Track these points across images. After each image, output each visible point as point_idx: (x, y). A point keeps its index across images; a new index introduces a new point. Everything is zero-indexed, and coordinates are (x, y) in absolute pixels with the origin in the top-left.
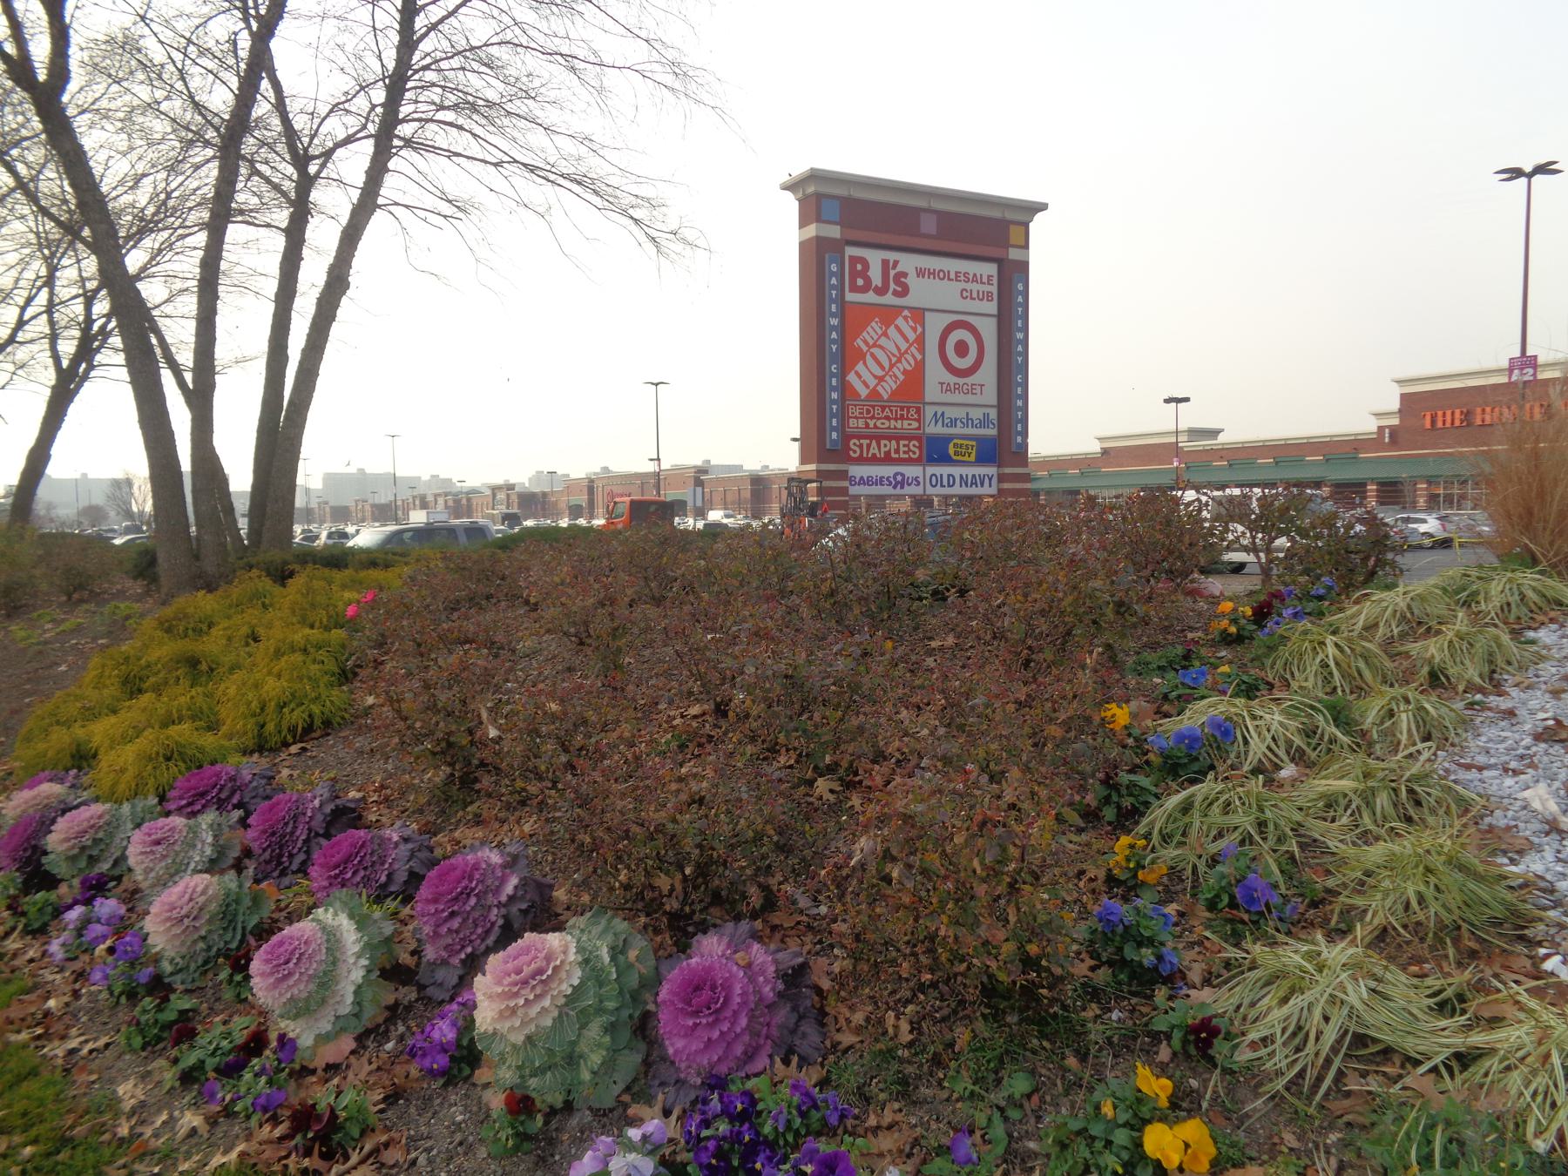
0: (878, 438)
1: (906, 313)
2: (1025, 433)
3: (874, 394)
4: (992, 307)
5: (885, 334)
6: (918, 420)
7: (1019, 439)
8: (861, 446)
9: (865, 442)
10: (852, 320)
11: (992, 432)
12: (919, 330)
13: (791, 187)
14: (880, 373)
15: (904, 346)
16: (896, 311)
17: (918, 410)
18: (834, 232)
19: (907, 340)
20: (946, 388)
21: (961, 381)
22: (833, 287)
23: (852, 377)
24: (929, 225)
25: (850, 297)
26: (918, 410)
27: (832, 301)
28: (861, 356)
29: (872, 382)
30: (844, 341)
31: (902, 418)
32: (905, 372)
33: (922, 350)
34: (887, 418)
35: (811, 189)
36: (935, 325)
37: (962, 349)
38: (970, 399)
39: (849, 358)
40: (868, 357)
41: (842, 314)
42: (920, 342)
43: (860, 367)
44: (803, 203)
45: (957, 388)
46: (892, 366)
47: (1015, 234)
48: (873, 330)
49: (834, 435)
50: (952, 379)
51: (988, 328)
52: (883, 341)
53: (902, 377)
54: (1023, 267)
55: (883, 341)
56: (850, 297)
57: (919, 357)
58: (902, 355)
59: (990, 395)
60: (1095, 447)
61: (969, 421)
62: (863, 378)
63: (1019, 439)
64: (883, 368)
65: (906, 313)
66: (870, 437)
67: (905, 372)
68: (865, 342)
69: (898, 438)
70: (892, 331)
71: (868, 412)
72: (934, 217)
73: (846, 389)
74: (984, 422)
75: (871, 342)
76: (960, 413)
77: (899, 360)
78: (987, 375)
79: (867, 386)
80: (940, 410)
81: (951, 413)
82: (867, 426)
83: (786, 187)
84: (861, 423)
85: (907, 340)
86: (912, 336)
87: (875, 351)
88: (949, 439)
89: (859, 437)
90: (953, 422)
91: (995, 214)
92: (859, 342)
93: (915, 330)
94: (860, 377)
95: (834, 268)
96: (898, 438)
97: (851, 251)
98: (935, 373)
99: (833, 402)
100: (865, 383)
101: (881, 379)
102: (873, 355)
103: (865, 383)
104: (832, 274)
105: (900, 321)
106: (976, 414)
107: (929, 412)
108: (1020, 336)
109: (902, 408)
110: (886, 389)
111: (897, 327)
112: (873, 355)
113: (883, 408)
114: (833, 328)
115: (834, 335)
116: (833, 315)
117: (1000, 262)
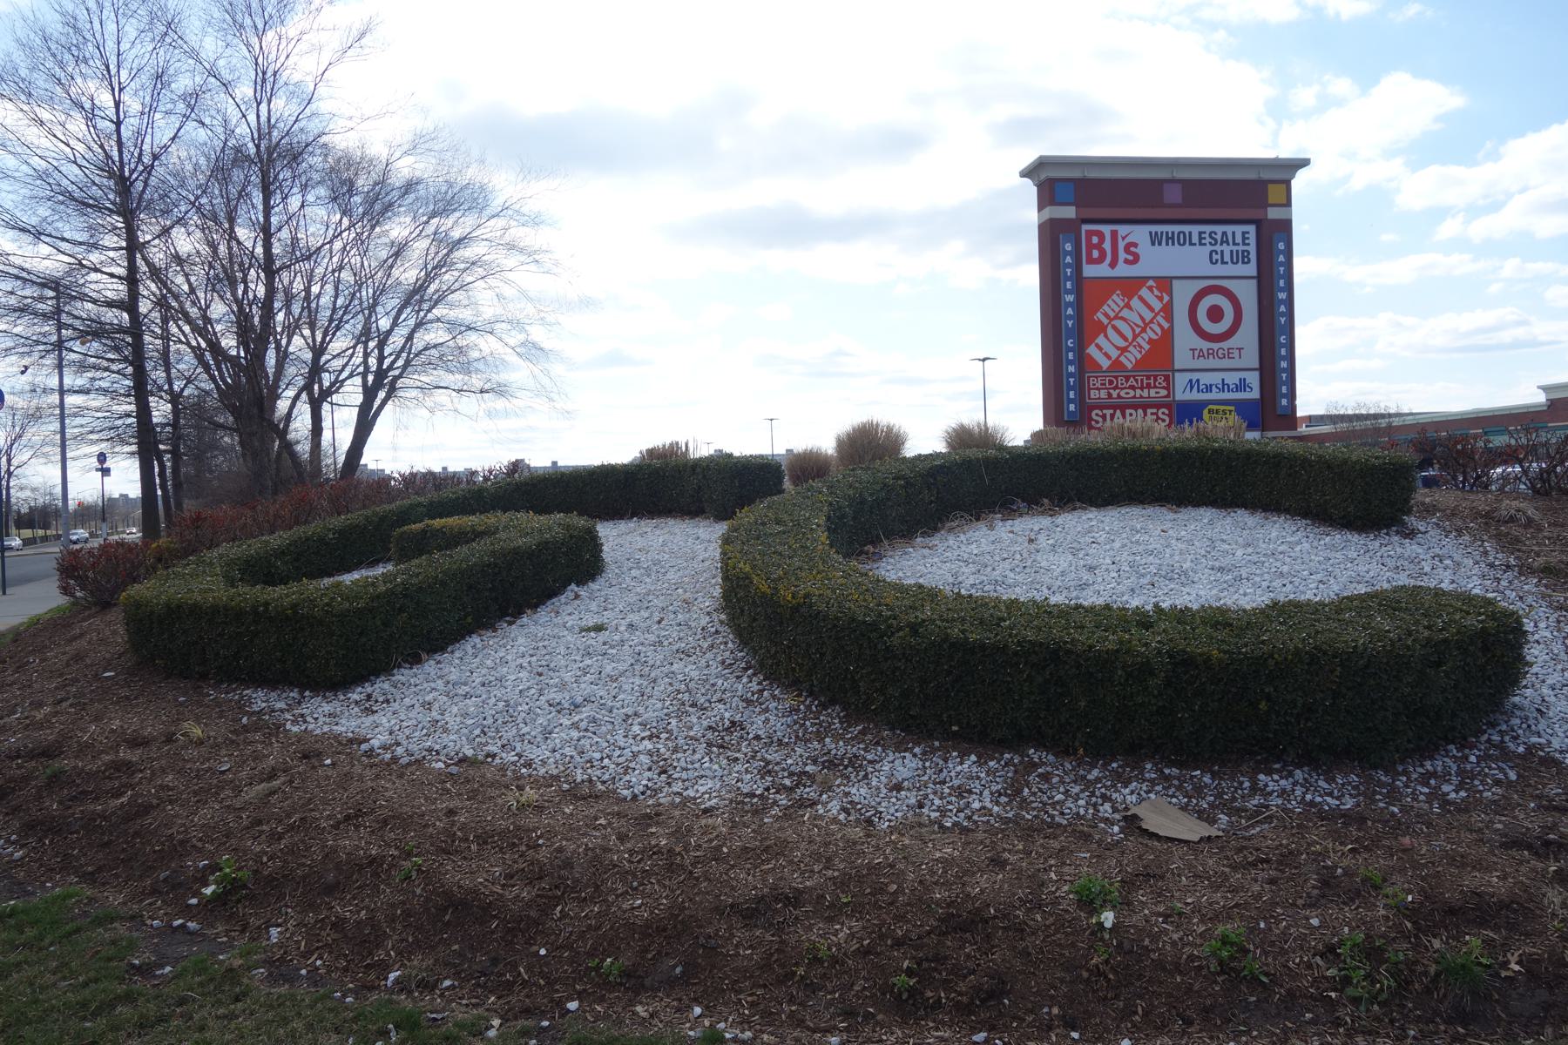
0: (1123, 408)
1: (1151, 283)
2: (1292, 395)
3: (1117, 365)
4: (1251, 269)
5: (1128, 306)
6: (1167, 388)
7: (1284, 402)
8: (1104, 417)
9: (1108, 412)
10: (1090, 294)
11: (1255, 394)
12: (1166, 298)
14: (1122, 344)
15: (1148, 315)
16: (1141, 281)
17: (1167, 378)
18: (1069, 212)
19: (1152, 309)
20: (1198, 354)
21: (1215, 346)
23: (1092, 350)
24: (1173, 195)
25: (1089, 271)
26: (1167, 378)
29: (1114, 354)
31: (1149, 386)
32: (1150, 341)
33: (1169, 316)
34: (1132, 387)
35: (1043, 177)
36: (1182, 295)
37: (1215, 314)
38: (1226, 363)
39: (1086, 331)
40: (1110, 331)
42: (1168, 311)
43: (1101, 340)
44: (1041, 187)
45: (1211, 353)
47: (1274, 193)
48: (1115, 302)
49: (1072, 407)
50: (1205, 345)
51: (1247, 294)
52: (1125, 313)
53: (1147, 347)
54: (1285, 227)
55: (1125, 313)
57: (1166, 325)
58: (1146, 325)
59: (1251, 357)
61: (1224, 386)
62: (1103, 350)
63: (1284, 402)
64: (1125, 339)
66: (1114, 407)
67: (1150, 341)
68: (1106, 315)
69: (1145, 407)
70: (1135, 302)
71: (1111, 382)
72: (1178, 187)
73: (1084, 362)
74: (1242, 386)
75: (1112, 315)
76: (1214, 378)
77: (1144, 330)
78: (1248, 336)
79: (1109, 357)
80: (1195, 376)
81: (1206, 379)
82: (1110, 396)
84: (1103, 394)
85: (1152, 309)
86: (1157, 305)
88: (1205, 404)
89: (1101, 408)
90: (1209, 388)
91: (1251, 175)
92: (1100, 315)
93: (1160, 299)
94: (1098, 346)
95: (1068, 247)
96: (1145, 407)
97: (1085, 227)
98: (1185, 341)
99: (1070, 375)
100: (1106, 354)
101: (1124, 350)
102: (1114, 327)
103: (1106, 354)
105: (1144, 292)
106: (1232, 379)
107: (1181, 380)
108: (1282, 296)
109: (1148, 378)
110: (1129, 361)
111: (1141, 299)
112: (1114, 327)
113: (1127, 378)
114: (1069, 304)
115: (1070, 311)
116: (1068, 292)
117: (1258, 223)
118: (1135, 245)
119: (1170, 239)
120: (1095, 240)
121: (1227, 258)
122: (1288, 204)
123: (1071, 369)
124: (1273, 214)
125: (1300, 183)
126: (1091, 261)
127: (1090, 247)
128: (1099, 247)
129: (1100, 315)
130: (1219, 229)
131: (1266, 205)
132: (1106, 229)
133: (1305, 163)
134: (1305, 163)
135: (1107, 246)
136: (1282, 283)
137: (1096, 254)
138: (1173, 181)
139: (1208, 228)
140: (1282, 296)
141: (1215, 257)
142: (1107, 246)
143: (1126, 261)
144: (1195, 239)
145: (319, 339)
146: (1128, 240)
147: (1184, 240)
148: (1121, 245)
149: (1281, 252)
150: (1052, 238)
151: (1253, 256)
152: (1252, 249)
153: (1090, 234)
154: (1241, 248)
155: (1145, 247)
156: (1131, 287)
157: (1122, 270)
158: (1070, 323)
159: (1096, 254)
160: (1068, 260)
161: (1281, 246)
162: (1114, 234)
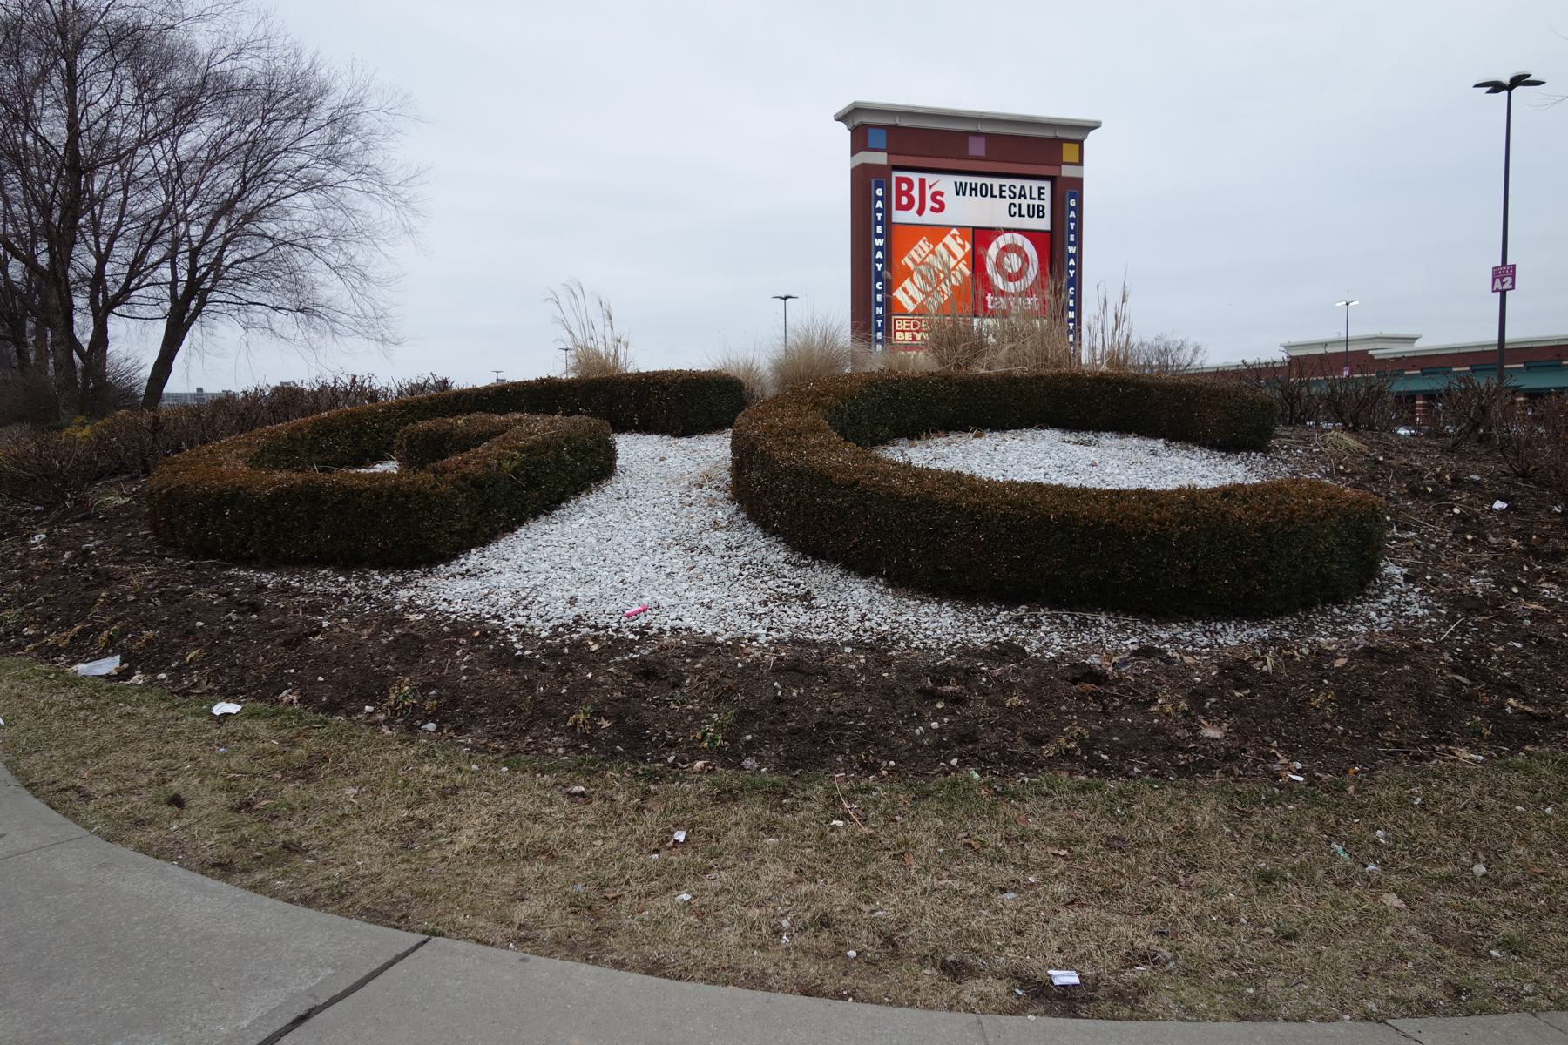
1: (954, 231)
13: (842, 118)
18: (881, 158)
22: (879, 210)
23: (898, 294)
24: (977, 148)
25: (899, 216)
27: (878, 223)
28: (908, 273)
29: (919, 298)
30: (888, 262)
32: (953, 287)
41: (886, 234)
43: (907, 283)
46: (939, 282)
47: (1069, 152)
54: (1078, 182)
56: (899, 216)
60: (1278, 356)
65: (954, 231)
67: (953, 287)
68: (913, 260)
70: (940, 247)
72: (983, 140)
73: (890, 305)
82: (914, 338)
83: (842, 118)
84: (908, 336)
87: (922, 268)
91: (1048, 134)
92: (906, 260)
93: (963, 247)
94: (905, 290)
95: (879, 192)
97: (896, 174)
102: (920, 272)
104: (878, 198)
105: (948, 240)
108: (1072, 250)
111: (945, 245)
112: (920, 272)
114: (878, 248)
115: (879, 255)
116: (879, 236)
117: (1053, 179)
118: (941, 194)
119: (973, 189)
120: (904, 187)
121: (1024, 212)
122: (1080, 163)
123: (880, 311)
124: (1067, 171)
125: (1091, 142)
126: (900, 207)
127: (900, 193)
128: (908, 193)
129: (906, 260)
130: (1018, 183)
131: (1059, 163)
132: (915, 177)
133: (1094, 126)
134: (1094, 126)
135: (915, 193)
136: (1072, 238)
137: (904, 200)
138: (977, 134)
139: (1008, 182)
140: (1072, 250)
141: (1014, 210)
142: (915, 193)
143: (933, 209)
144: (996, 192)
145: (103, 247)
146: (934, 189)
147: (986, 192)
148: (929, 193)
149: (1072, 208)
150: (864, 182)
151: (1047, 211)
152: (1047, 204)
153: (899, 181)
154: (1037, 202)
155: (950, 197)
156: (936, 233)
157: (929, 218)
158: (879, 266)
159: (904, 200)
160: (879, 205)
161: (1073, 203)
162: (922, 182)
